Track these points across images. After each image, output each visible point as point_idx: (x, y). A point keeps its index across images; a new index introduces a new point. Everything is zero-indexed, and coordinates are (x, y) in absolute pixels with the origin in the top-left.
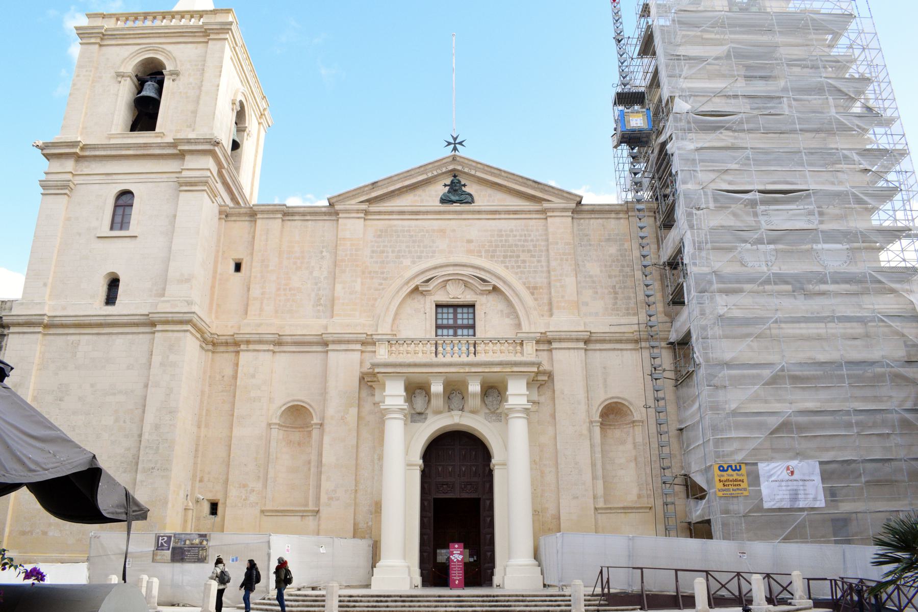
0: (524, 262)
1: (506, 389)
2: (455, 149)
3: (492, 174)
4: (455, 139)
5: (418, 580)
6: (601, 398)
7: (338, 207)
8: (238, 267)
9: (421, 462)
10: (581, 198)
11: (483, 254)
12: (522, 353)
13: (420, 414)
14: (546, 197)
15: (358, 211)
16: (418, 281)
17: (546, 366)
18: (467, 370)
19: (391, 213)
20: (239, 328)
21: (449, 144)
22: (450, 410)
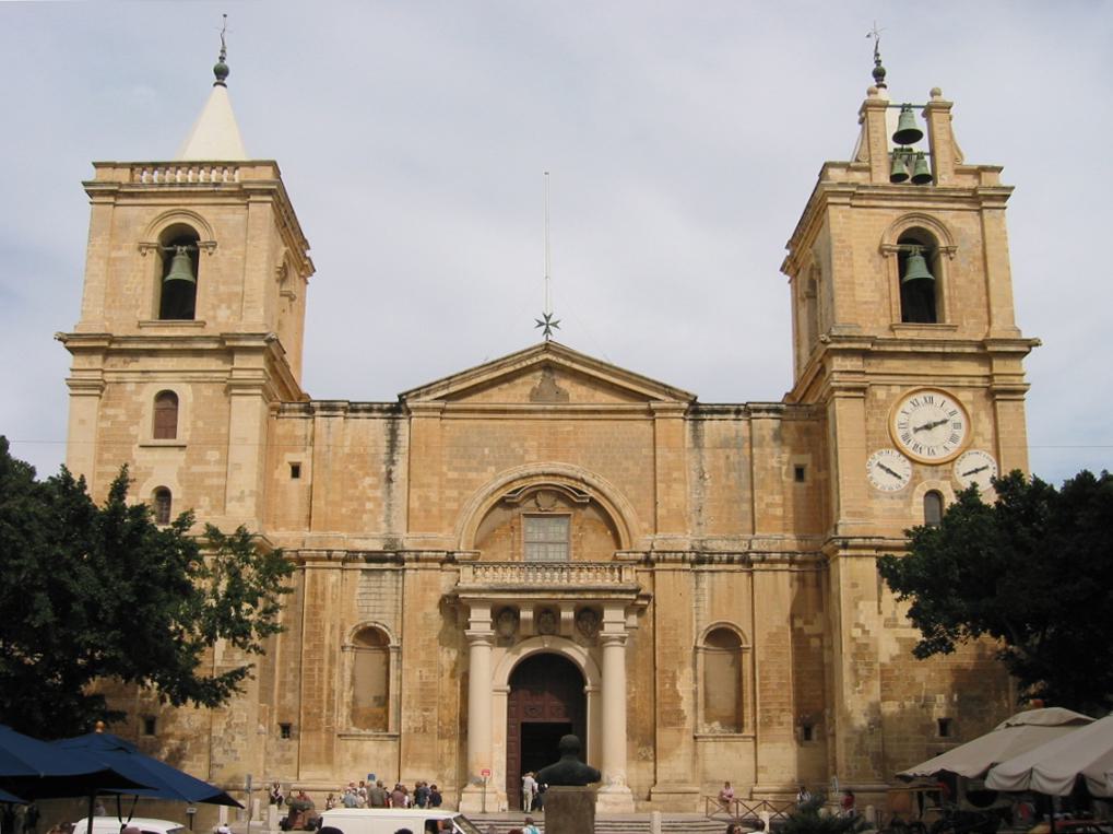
0: (627, 470)
1: (601, 615)
2: (547, 331)
3: (594, 368)
4: (547, 318)
5: (505, 805)
6: (706, 622)
7: (410, 404)
8: (296, 471)
9: (508, 688)
10: (696, 398)
11: (579, 460)
12: (620, 579)
13: (507, 638)
14: (660, 396)
15: (434, 409)
16: (503, 493)
17: (646, 590)
18: (560, 596)
19: (472, 411)
20: (303, 544)
21: (541, 324)
22: (541, 634)
